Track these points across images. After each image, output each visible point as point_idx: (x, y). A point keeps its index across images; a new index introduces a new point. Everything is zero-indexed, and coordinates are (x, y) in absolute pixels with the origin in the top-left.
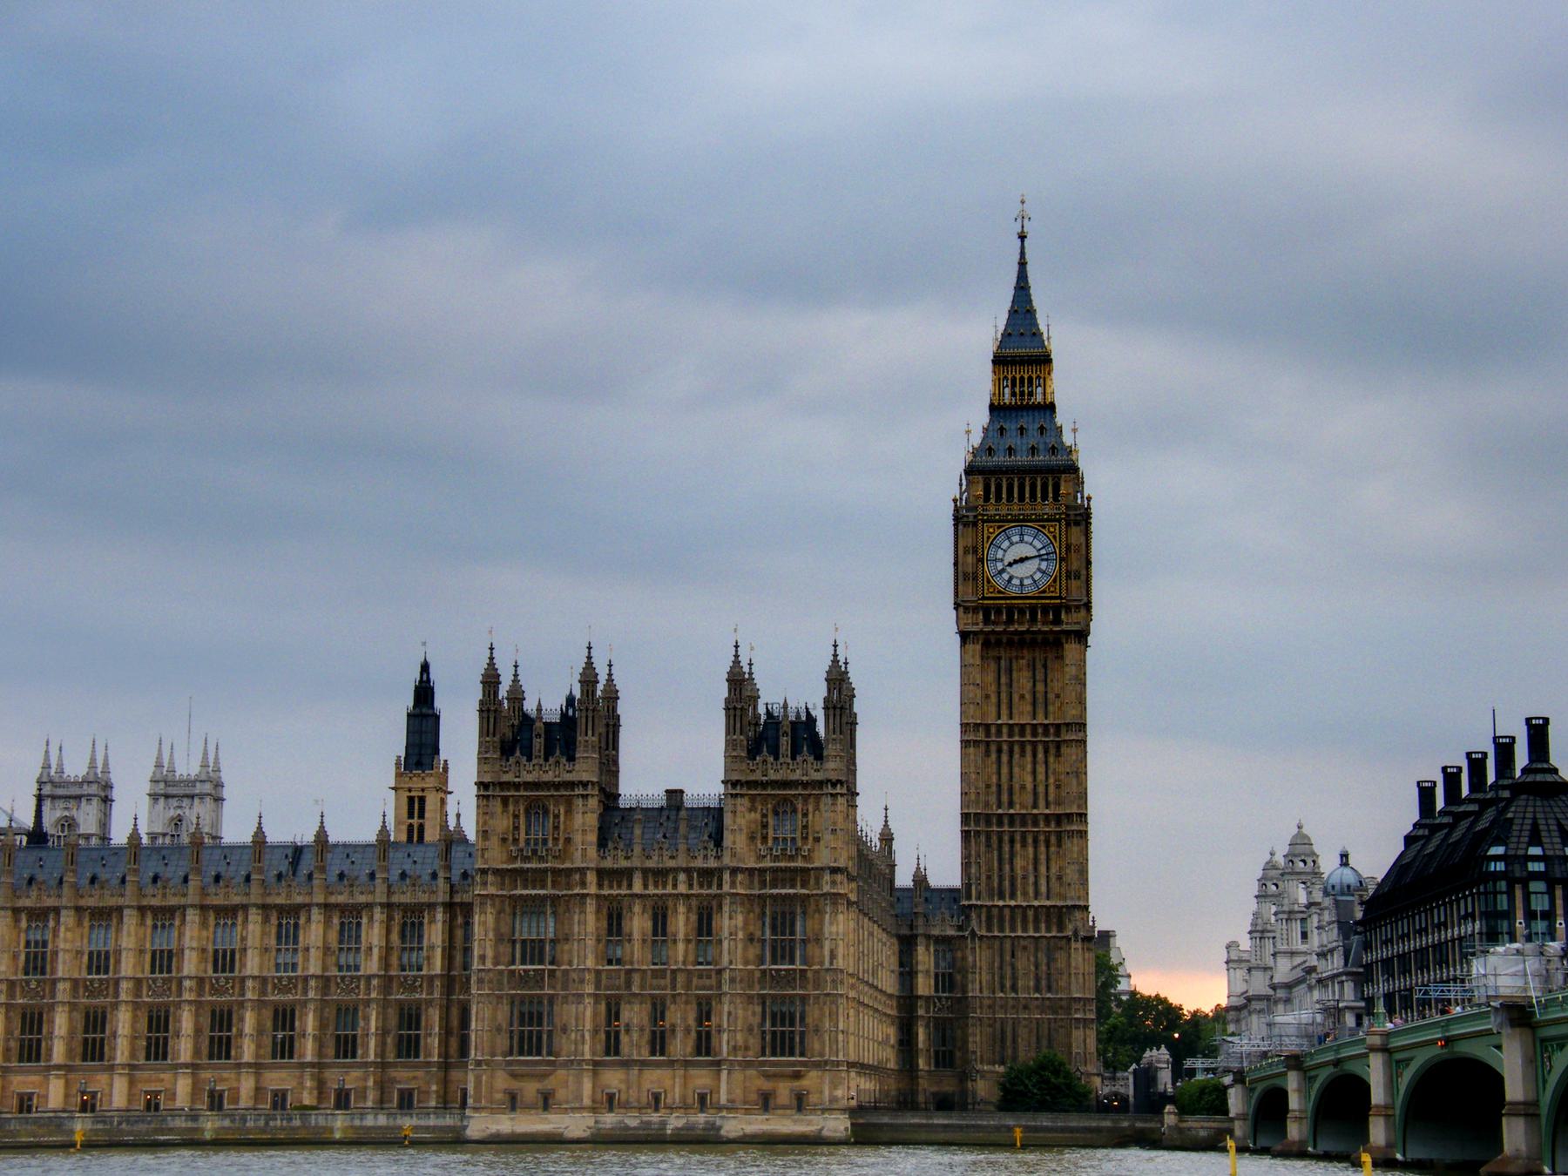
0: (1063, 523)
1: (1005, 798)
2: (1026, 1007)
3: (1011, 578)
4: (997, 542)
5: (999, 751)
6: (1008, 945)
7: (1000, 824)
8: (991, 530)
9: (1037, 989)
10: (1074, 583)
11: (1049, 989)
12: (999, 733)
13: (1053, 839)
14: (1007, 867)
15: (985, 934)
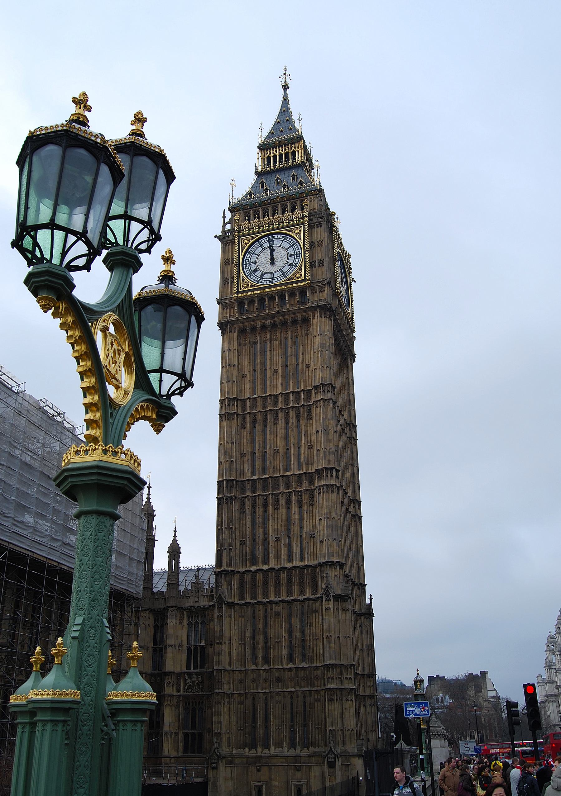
0: (306, 224)
1: (259, 463)
2: (278, 680)
3: (263, 274)
4: (252, 249)
5: (254, 422)
6: (260, 613)
7: (254, 489)
8: (246, 242)
9: (291, 659)
10: (318, 270)
11: (304, 657)
12: (254, 406)
13: (305, 497)
14: (260, 531)
15: (236, 601)
